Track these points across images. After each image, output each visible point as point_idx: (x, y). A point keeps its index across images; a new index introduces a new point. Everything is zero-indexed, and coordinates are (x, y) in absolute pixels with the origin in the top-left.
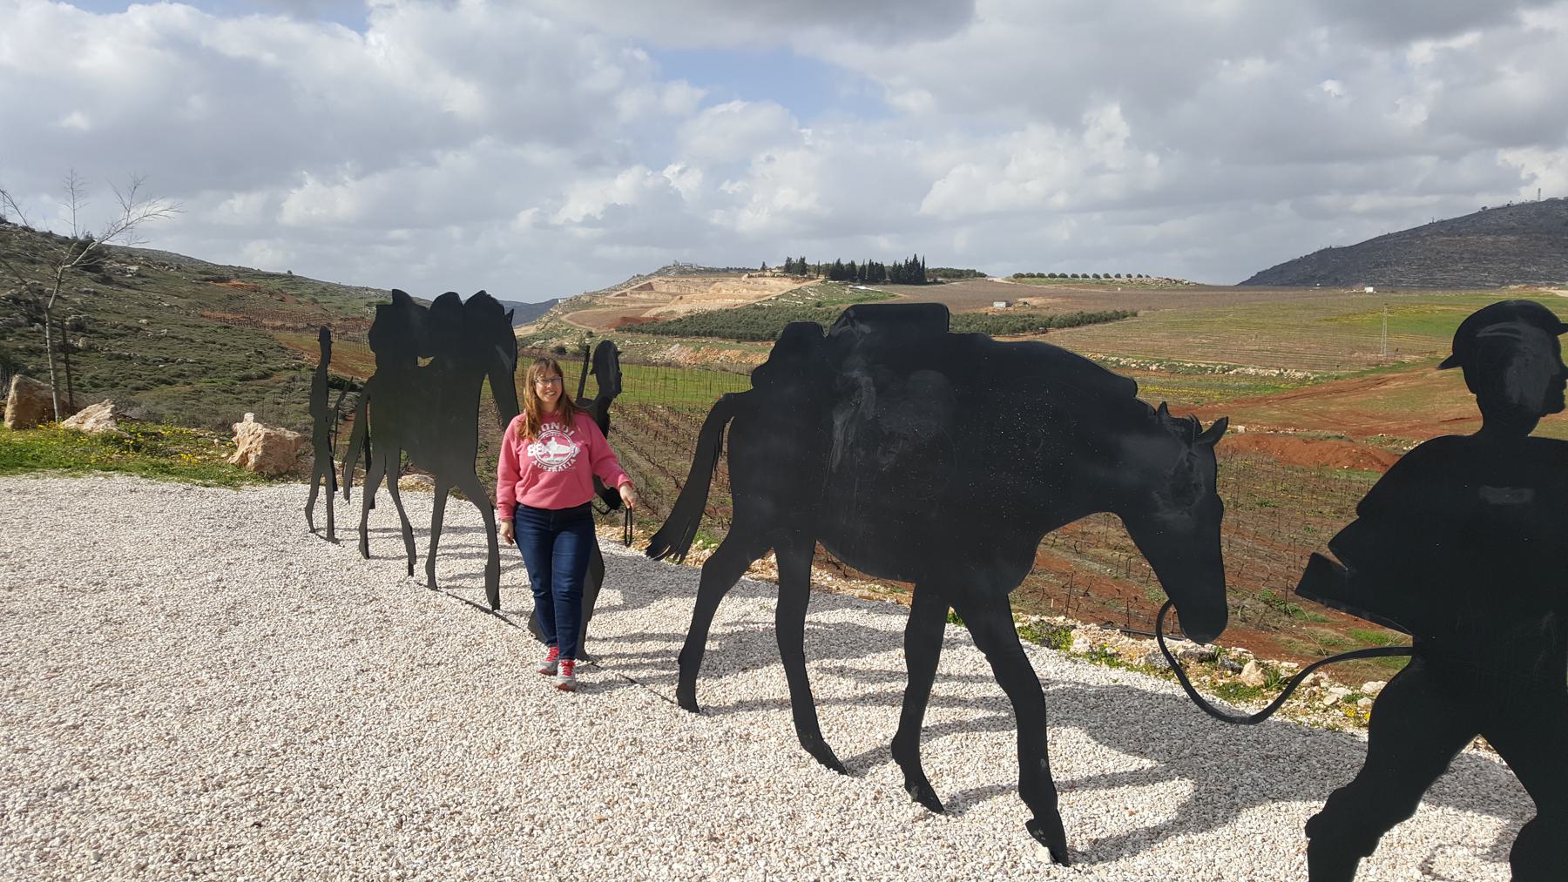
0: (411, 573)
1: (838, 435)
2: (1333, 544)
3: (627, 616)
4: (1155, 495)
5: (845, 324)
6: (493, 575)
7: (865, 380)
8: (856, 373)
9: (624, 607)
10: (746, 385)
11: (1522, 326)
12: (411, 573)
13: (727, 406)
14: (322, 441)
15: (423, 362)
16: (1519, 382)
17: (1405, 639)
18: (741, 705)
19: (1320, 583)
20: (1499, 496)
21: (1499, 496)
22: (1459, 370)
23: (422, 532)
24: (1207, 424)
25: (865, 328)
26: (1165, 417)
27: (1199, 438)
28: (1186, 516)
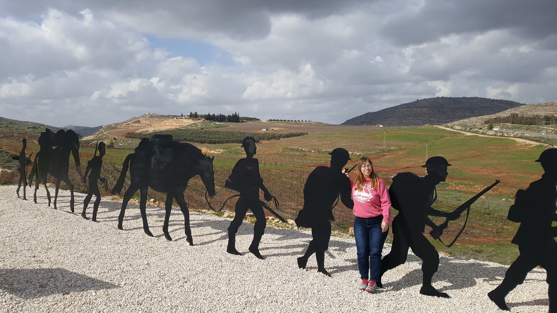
0: (49, 206)
1: (152, 162)
3: (109, 213)
6: (72, 202)
7: (157, 150)
9: (109, 212)
12: (49, 206)
13: (129, 157)
14: (22, 170)
15: (54, 148)
18: (134, 228)
20: (249, 168)
21: (249, 168)
23: (53, 197)
25: (157, 139)
27: (210, 159)
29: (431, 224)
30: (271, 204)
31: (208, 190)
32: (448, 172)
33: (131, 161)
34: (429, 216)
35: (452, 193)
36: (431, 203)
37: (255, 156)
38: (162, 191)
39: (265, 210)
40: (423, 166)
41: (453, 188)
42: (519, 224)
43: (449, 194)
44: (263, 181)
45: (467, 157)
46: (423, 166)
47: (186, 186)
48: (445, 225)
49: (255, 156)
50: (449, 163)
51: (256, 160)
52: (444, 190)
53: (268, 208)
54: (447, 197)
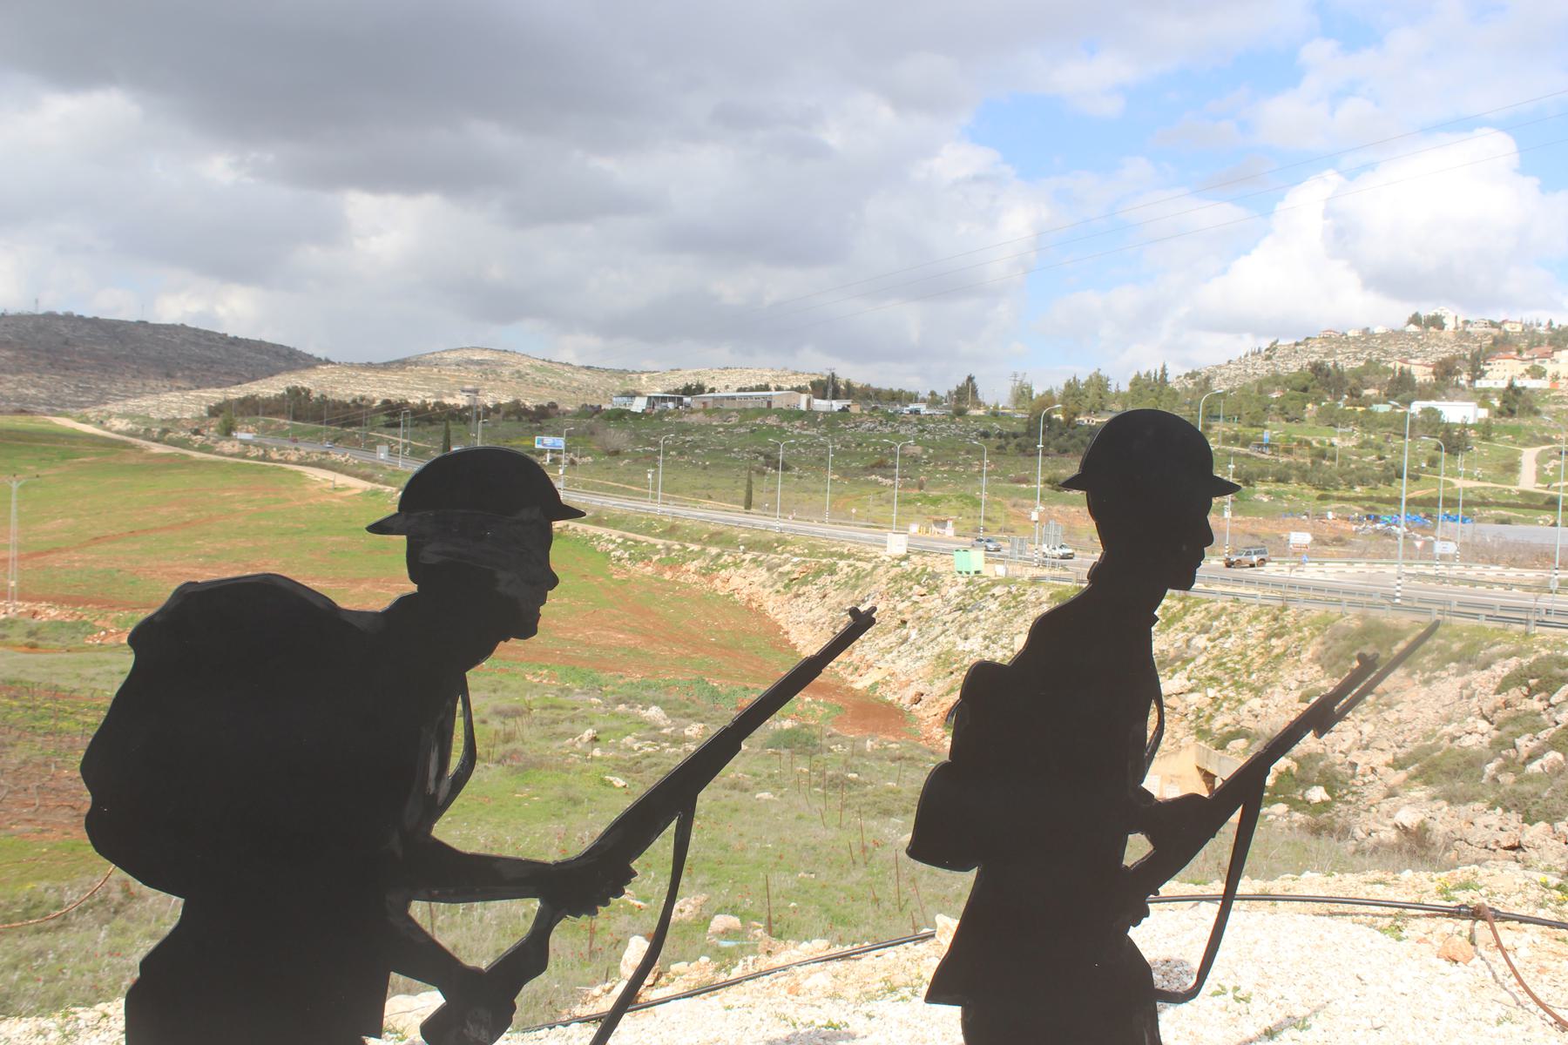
29: (432, 964)
32: (558, 557)
34: (418, 910)
36: (436, 808)
40: (379, 528)
41: (111, 640)
42: (970, 876)
45: (155, 530)
46: (379, 528)
48: (529, 958)
50: (567, 497)
52: (79, 650)
54: (90, 672)
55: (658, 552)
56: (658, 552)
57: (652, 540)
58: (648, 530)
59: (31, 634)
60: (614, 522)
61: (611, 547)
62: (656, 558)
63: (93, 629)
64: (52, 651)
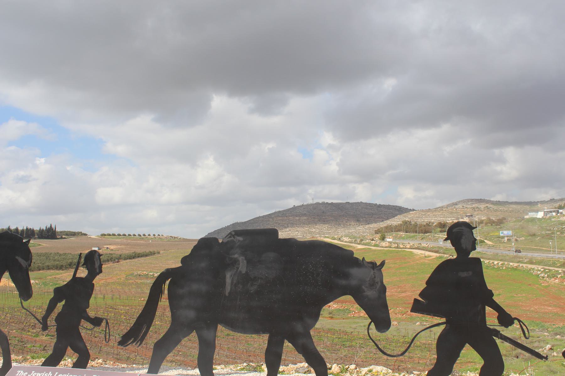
1: (228, 280)
2: (421, 295)
4: (363, 287)
5: (230, 237)
7: (241, 259)
8: (236, 256)
10: (180, 265)
11: (463, 228)
16: (465, 243)
17: (444, 320)
19: (417, 307)
20: (464, 275)
21: (464, 275)
22: (449, 241)
24: (378, 264)
26: (364, 262)
27: (377, 267)
28: (375, 292)
30: (513, 331)
31: (374, 319)
33: (173, 281)
35: (357, 320)
37: (473, 255)
38: (257, 331)
39: (498, 341)
41: (356, 315)
43: (354, 323)
44: (493, 295)
47: (316, 317)
49: (473, 255)
51: (477, 261)
52: (346, 319)
53: (505, 339)
54: (354, 326)
55: (560, 273)
56: (560, 273)
57: (557, 269)
58: (554, 265)
59: (330, 313)
60: (539, 263)
61: (539, 272)
62: (559, 276)
63: (350, 311)
64: (337, 319)
